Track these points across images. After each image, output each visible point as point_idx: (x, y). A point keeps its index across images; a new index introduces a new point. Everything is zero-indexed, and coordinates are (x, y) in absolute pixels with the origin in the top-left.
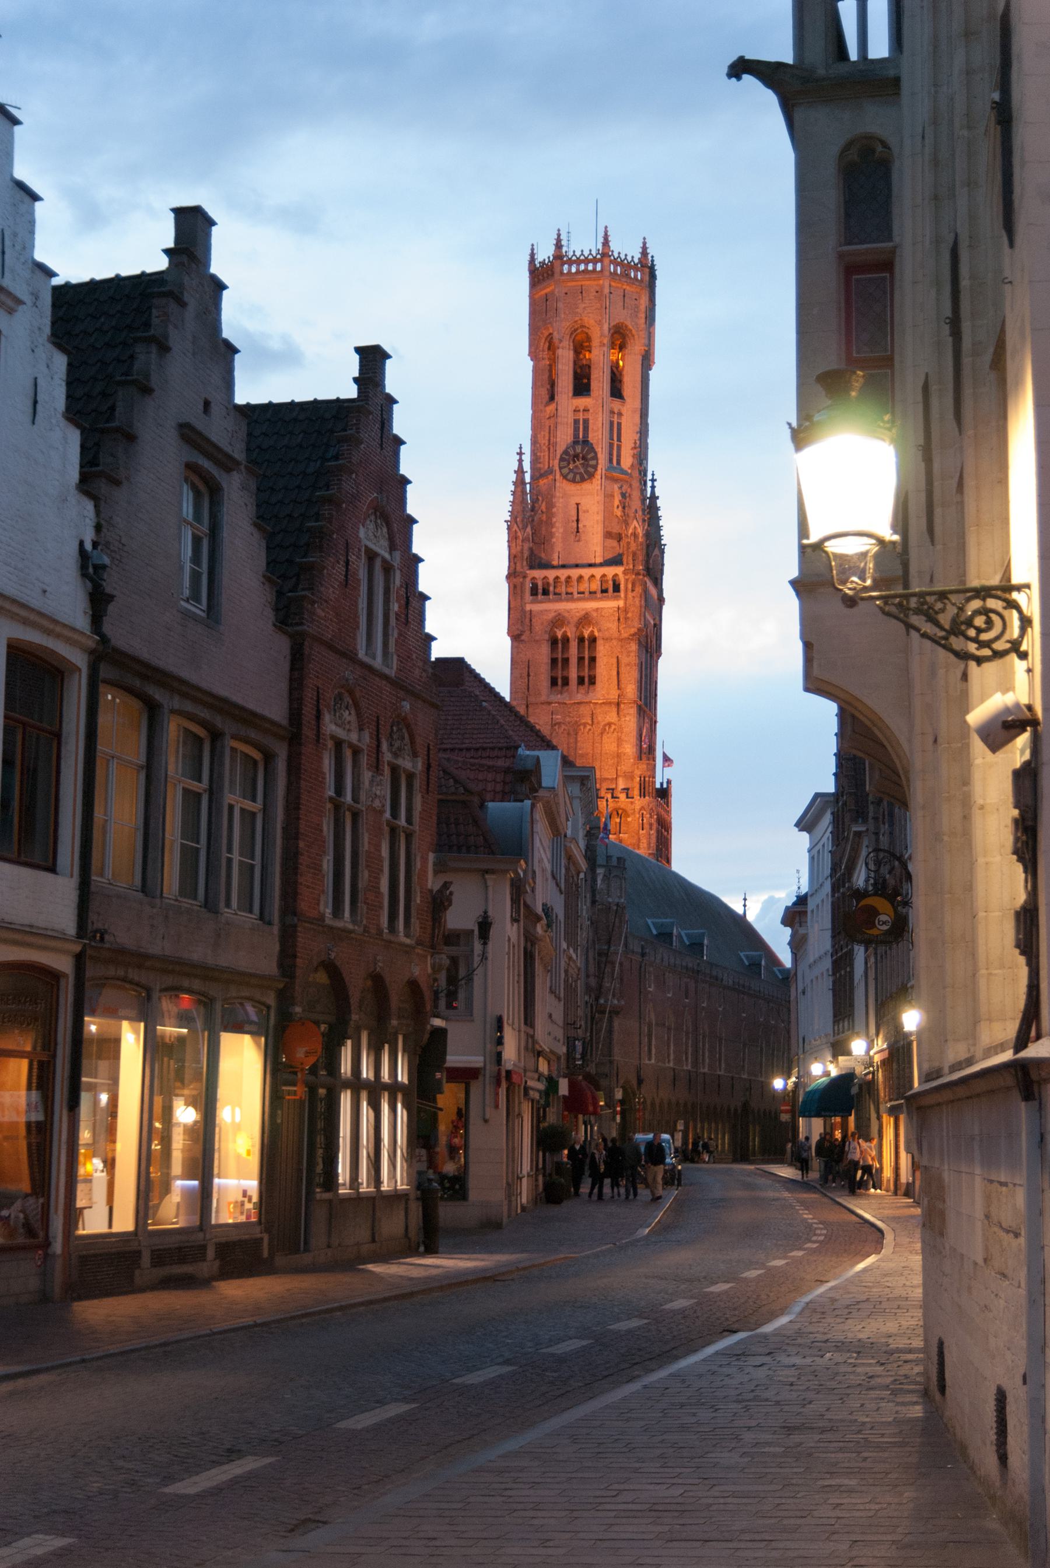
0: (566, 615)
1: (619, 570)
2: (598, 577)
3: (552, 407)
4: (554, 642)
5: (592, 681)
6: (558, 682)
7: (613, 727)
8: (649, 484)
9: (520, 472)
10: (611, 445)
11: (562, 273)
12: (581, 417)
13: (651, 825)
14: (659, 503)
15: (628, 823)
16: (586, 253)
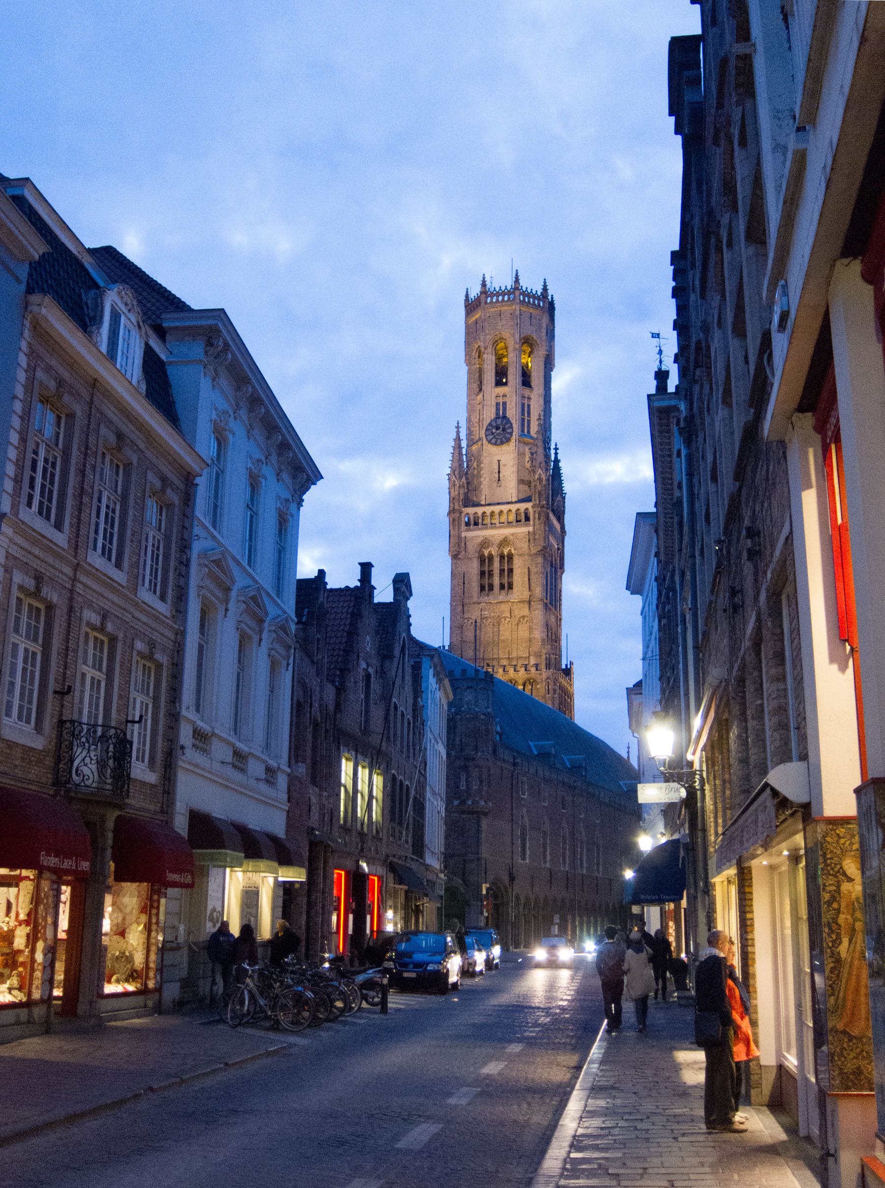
0: (491, 539)
1: (529, 505)
2: (514, 511)
3: (480, 396)
4: (482, 560)
5: (510, 586)
6: (485, 588)
7: (526, 619)
8: (553, 452)
9: (458, 440)
10: (523, 420)
11: (486, 303)
12: (501, 400)
13: (555, 690)
14: (560, 464)
15: (538, 689)
16: (503, 289)
